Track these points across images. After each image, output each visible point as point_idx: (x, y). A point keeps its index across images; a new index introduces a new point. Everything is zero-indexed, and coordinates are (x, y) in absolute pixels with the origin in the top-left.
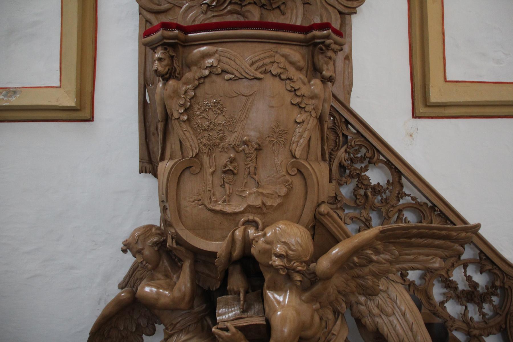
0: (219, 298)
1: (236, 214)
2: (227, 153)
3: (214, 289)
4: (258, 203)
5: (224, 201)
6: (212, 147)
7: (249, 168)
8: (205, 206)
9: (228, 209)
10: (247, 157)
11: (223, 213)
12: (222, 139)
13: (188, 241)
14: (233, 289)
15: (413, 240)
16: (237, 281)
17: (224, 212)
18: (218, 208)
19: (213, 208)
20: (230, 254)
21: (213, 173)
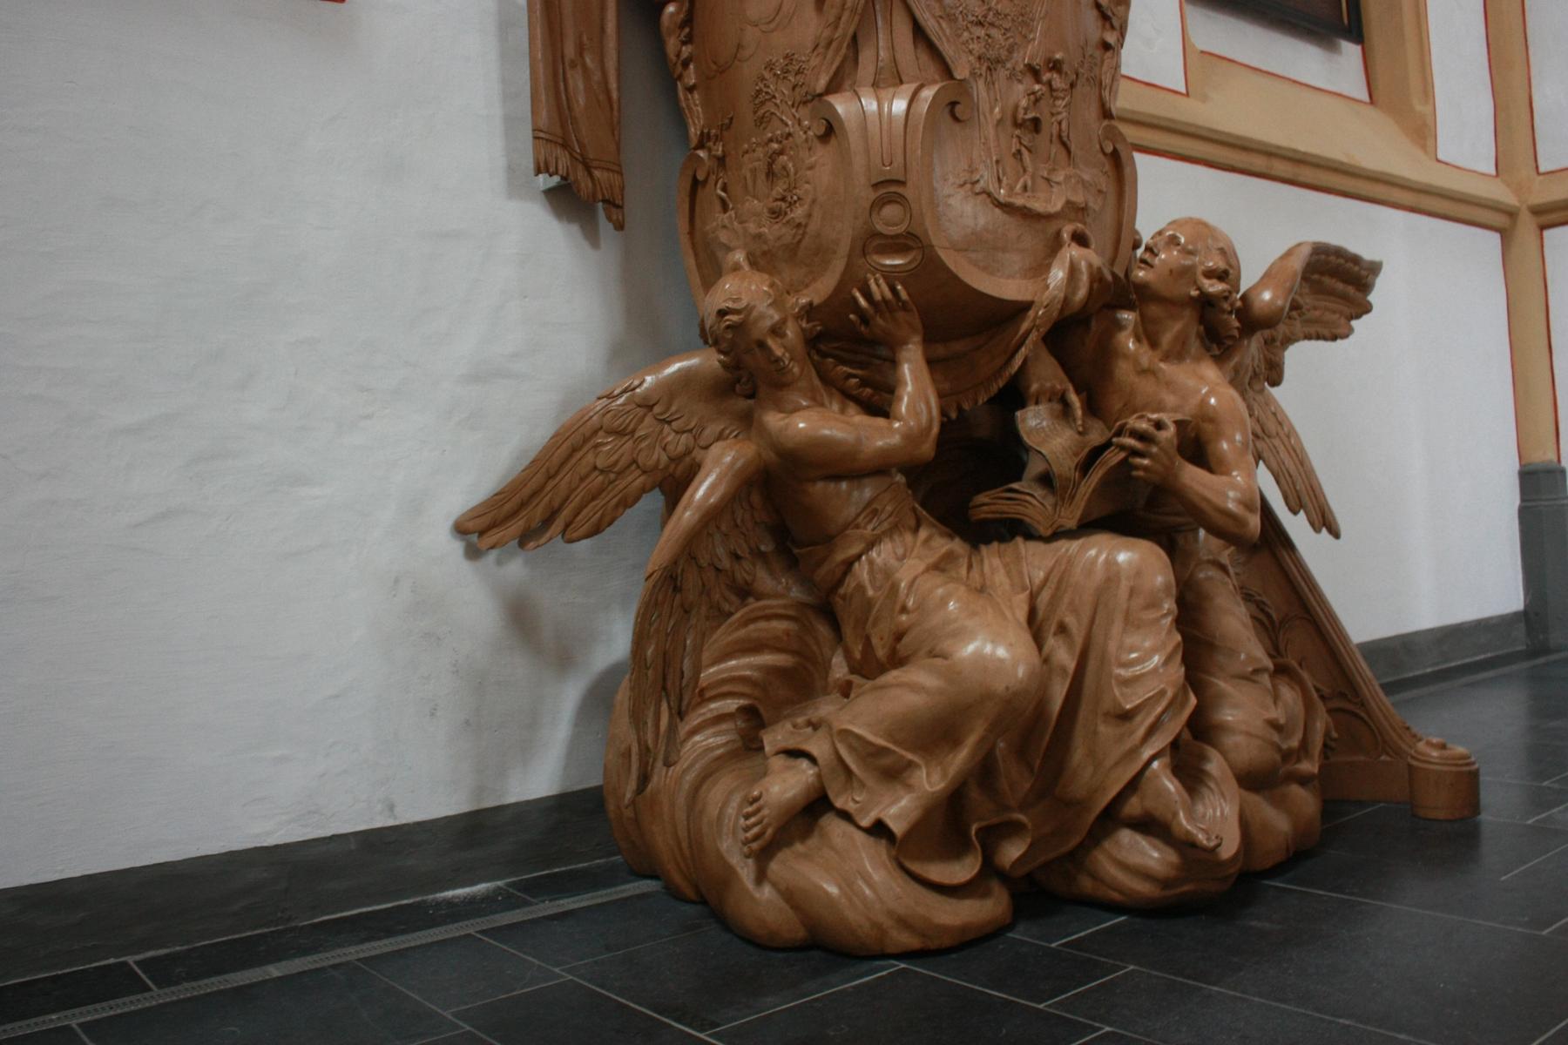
0: (1018, 414)
1: (1049, 217)
2: (1020, 81)
3: (954, 415)
4: (1079, 198)
5: (1025, 188)
6: (993, 64)
7: (1060, 123)
8: (989, 195)
9: (1038, 206)
10: (1057, 98)
11: (1026, 214)
12: (1010, 51)
13: (960, 275)
14: (1053, 387)
15: (1327, 280)
16: (1047, 374)
17: (1030, 210)
18: (1019, 201)
19: (1011, 200)
20: (1066, 299)
21: (1000, 122)
